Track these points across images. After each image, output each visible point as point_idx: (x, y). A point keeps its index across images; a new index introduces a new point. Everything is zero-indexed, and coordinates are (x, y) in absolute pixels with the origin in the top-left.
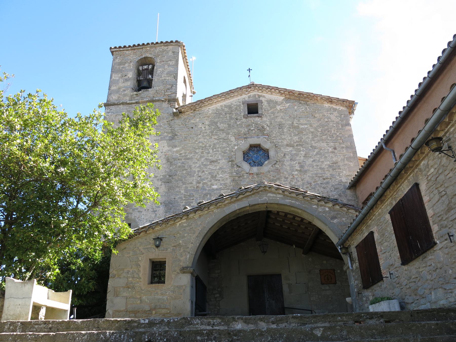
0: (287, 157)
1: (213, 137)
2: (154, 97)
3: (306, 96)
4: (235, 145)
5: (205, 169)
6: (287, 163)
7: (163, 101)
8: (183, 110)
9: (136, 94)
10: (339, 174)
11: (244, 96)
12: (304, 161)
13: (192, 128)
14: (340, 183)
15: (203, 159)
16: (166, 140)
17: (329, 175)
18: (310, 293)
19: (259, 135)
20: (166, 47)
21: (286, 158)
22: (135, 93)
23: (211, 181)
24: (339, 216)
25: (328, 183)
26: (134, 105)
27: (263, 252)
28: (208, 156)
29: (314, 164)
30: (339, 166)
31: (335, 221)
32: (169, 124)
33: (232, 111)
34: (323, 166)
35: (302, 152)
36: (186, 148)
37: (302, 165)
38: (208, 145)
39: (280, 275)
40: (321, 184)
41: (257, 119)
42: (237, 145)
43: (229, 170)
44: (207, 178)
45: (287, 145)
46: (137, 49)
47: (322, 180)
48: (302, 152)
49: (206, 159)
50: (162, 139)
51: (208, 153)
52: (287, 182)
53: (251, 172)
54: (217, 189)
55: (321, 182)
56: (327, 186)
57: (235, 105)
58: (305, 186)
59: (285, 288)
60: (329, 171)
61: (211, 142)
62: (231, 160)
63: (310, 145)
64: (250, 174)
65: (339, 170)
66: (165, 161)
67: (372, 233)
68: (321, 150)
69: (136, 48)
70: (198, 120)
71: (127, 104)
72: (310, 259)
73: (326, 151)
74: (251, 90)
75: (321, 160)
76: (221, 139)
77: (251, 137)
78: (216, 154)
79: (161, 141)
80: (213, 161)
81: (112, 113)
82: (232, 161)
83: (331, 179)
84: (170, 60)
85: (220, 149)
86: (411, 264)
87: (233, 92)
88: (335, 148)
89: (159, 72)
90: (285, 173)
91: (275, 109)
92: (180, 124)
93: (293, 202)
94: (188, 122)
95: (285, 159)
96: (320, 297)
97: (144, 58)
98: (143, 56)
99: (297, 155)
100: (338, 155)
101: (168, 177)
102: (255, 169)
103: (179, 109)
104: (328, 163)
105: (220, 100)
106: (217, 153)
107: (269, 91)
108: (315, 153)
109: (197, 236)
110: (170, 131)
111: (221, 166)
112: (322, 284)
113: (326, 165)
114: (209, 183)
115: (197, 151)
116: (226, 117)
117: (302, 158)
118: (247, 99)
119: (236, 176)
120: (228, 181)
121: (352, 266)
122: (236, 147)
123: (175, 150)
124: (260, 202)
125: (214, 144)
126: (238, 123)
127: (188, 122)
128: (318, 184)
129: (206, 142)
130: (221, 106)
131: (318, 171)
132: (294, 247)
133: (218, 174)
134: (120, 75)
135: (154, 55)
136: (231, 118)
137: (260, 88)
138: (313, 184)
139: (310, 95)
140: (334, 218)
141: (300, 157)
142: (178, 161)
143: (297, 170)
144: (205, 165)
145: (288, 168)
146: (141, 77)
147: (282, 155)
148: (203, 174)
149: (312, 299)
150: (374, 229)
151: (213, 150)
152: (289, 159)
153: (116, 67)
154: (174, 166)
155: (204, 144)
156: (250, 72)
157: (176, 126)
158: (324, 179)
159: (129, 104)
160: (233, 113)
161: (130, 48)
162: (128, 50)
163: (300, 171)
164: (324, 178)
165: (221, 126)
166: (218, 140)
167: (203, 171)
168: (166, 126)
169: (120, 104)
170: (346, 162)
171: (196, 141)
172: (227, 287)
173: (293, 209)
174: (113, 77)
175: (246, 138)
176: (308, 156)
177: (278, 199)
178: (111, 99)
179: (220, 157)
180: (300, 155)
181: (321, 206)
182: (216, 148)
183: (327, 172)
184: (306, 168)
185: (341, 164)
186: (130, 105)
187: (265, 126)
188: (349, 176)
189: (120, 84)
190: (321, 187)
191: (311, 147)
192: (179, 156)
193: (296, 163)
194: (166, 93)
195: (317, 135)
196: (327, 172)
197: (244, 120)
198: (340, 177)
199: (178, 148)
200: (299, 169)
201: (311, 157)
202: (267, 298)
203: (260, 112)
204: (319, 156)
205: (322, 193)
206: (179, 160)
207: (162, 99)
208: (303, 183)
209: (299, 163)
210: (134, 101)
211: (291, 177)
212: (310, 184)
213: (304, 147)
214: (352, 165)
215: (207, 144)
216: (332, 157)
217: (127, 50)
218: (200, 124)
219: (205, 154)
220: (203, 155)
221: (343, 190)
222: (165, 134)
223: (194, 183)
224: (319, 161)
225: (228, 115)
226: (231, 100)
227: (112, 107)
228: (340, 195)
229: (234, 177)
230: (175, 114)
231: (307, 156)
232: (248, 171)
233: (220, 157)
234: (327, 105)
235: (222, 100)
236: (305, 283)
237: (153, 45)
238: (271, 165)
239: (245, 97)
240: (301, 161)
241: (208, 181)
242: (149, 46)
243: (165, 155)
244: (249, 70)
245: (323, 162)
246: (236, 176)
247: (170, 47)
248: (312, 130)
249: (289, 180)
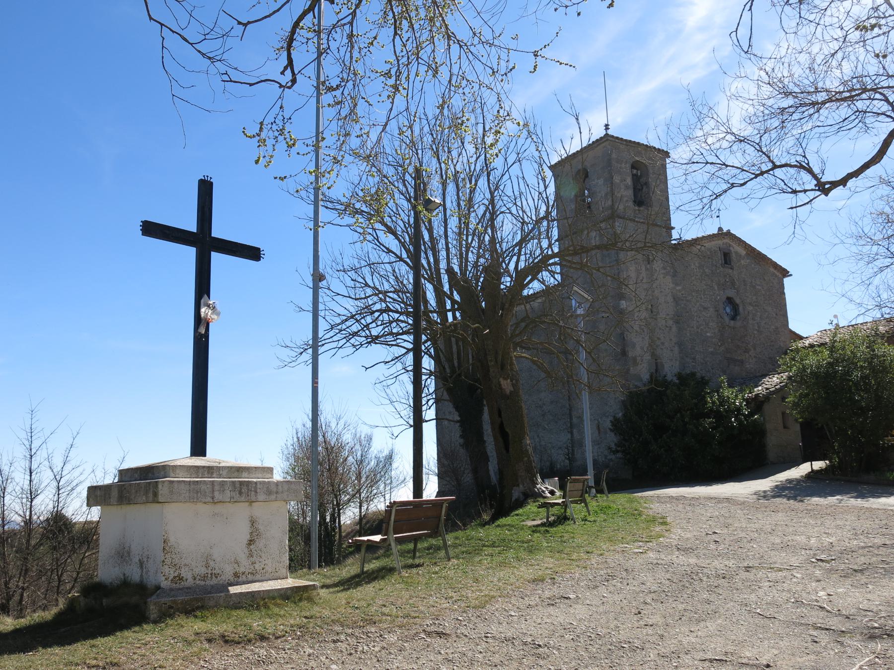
6: (751, 322)
15: (698, 304)
66: (672, 300)
114: (705, 330)
117: (759, 319)
120: (716, 331)
209: (757, 324)
212: (764, 344)
223: (695, 328)
234: (772, 269)
239: (719, 242)
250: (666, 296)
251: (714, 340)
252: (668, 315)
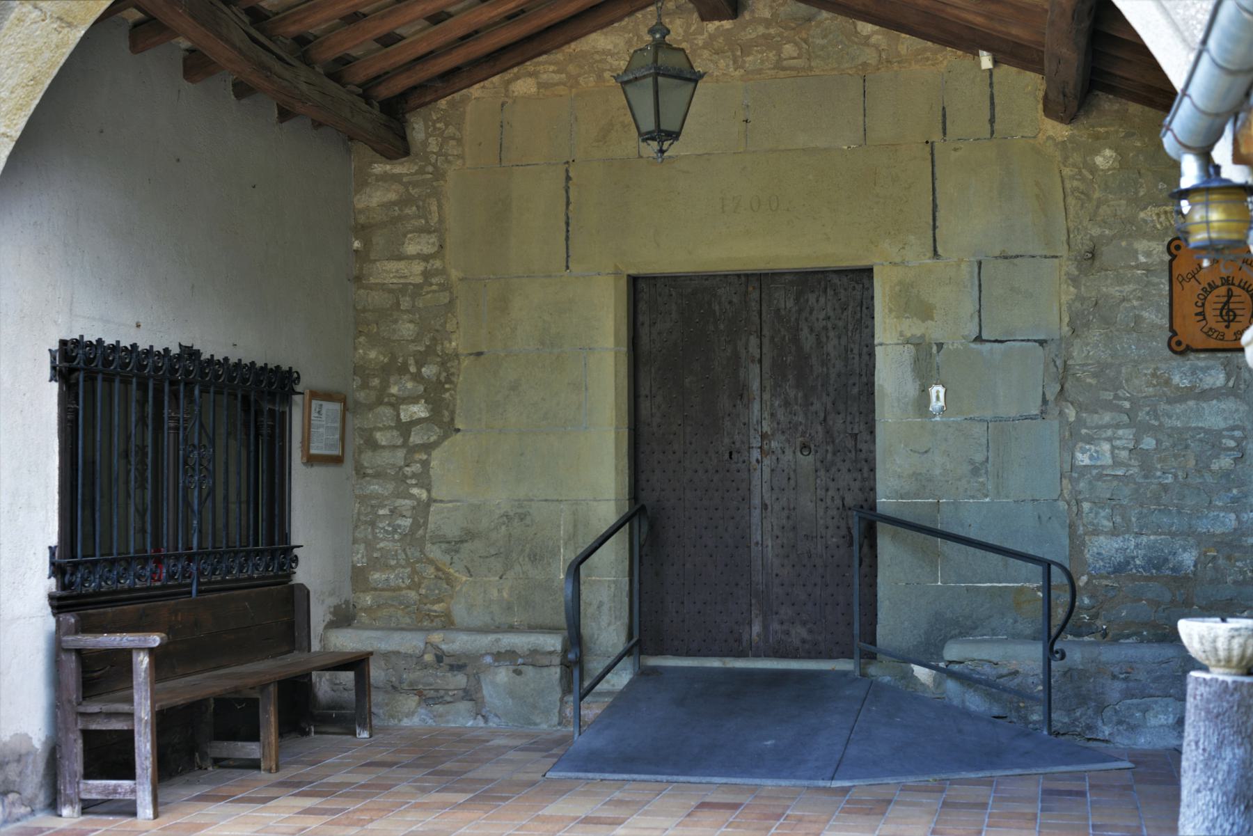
18: (1071, 413)
27: (647, 137)
72: (1104, 159)
96: (1149, 443)
112: (1179, 348)
132: (986, 61)
149: (1083, 459)
172: (479, 354)
202: (764, 436)
236: (1042, 343)
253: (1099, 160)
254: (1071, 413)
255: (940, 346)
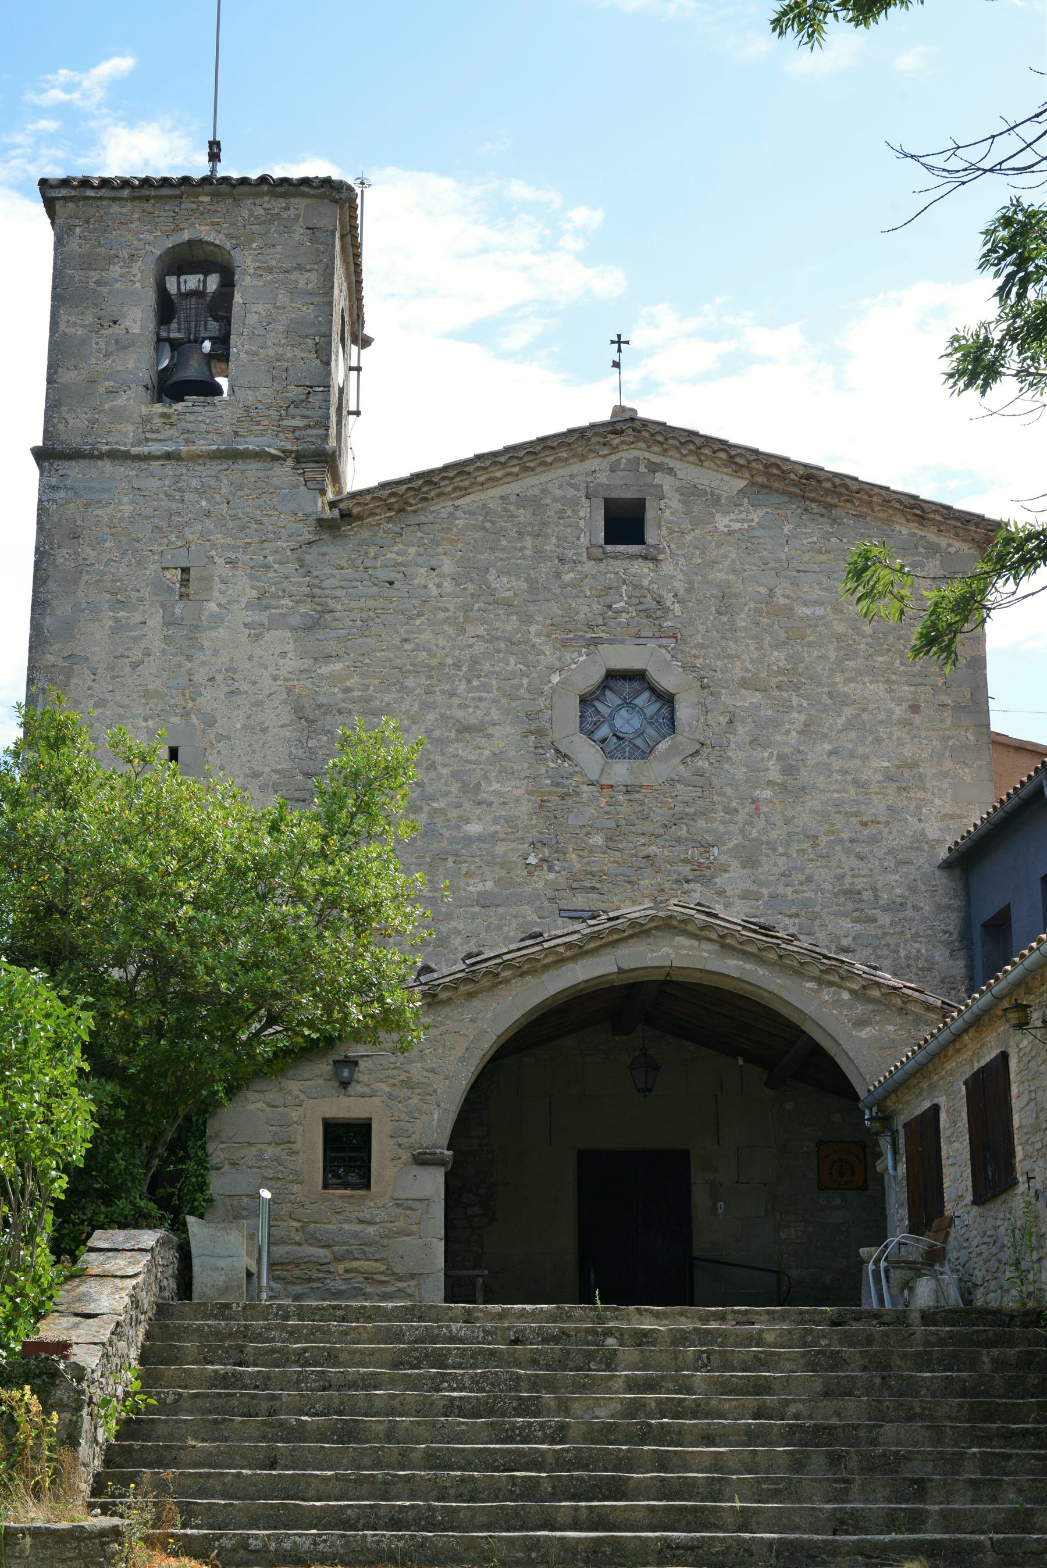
0: (740, 729)
1: (472, 629)
2: (236, 433)
3: (829, 485)
4: (553, 670)
5: (438, 759)
7: (274, 458)
8: (355, 511)
9: (164, 415)
10: (919, 808)
11: (593, 463)
12: (800, 752)
13: (391, 583)
14: (918, 841)
15: (430, 717)
16: (293, 629)
17: (882, 808)
18: (778, 1216)
19: (643, 634)
20: (282, 203)
21: (734, 733)
22: (159, 408)
23: (459, 806)
24: (878, 1018)
25: (874, 839)
26: (155, 465)
28: (450, 707)
29: (836, 764)
30: (921, 777)
31: (866, 1033)
32: (301, 561)
33: (544, 524)
34: (866, 774)
35: (795, 715)
36: (367, 665)
37: (791, 767)
38: (449, 661)
39: (686, 1153)
40: (851, 841)
41: (640, 568)
42: (561, 670)
43: (526, 766)
44: (447, 793)
45: (744, 684)
46: (155, 197)
47: (859, 827)
48: (795, 715)
49: (442, 716)
50: (276, 622)
51: (452, 694)
52: (733, 828)
53: (604, 782)
54: (480, 838)
55: (853, 835)
56: (871, 852)
57: (555, 500)
58: (796, 847)
59: (700, 1196)
60: (886, 795)
61: (461, 649)
62: (533, 728)
63: (826, 689)
64: (602, 787)
65: (921, 795)
66: (286, 715)
67: (935, 1109)
68: (864, 710)
69: (153, 192)
70: (412, 550)
71: (126, 456)
72: (789, 1106)
73: (882, 716)
74: (623, 442)
75: (861, 751)
76: (498, 638)
77: (611, 642)
78: (480, 699)
79: (272, 632)
80: (468, 729)
81: (71, 494)
82: (540, 733)
83: (887, 824)
84: (299, 268)
85: (494, 682)
86: (988, 1206)
87: (553, 448)
88: (915, 709)
89: (252, 319)
90: (729, 790)
91: (710, 527)
92: (343, 563)
93: (748, 966)
94: (376, 557)
95: (733, 738)
96: (810, 1229)
97: (190, 242)
98: (186, 236)
99: (775, 723)
100: (923, 734)
101: (300, 777)
102: (621, 771)
103: (343, 506)
104: (886, 764)
105: (499, 474)
106: (484, 695)
107: (691, 452)
108: (840, 722)
109: (462, 1059)
110: (306, 590)
111: (497, 751)
112: (822, 1187)
113: (875, 771)
115: (410, 682)
116: (522, 549)
118: (603, 478)
119: (551, 793)
120: (525, 807)
121: (895, 1168)
122: (556, 679)
123: (325, 670)
124: (650, 964)
125: (474, 661)
126: (568, 577)
127: (376, 557)
128: (841, 841)
129: (443, 648)
130: (502, 497)
131: (845, 791)
132: (740, 1062)
133: (486, 777)
134: (89, 319)
135: (229, 236)
136: (540, 554)
137: (660, 438)
138: (824, 838)
139: (845, 486)
140: (861, 1023)
141: (788, 732)
142: (339, 718)
143: (770, 783)
144: (438, 741)
145: (740, 773)
146: (174, 325)
147: (724, 720)
148: (432, 774)
149: (783, 1235)
150: (942, 1101)
151: (469, 681)
152: (748, 739)
153: (72, 277)
154: (325, 738)
155: (432, 656)
156: (619, 350)
157: (328, 571)
158: (864, 824)
159: (138, 458)
160: (549, 531)
161: (126, 193)
162: (121, 199)
163: (784, 787)
164: (865, 819)
165: (505, 585)
166: (486, 641)
167: (433, 766)
168: (290, 568)
169: (101, 456)
170: (948, 765)
171: (405, 640)
173: (744, 985)
174: (63, 326)
175: (595, 642)
176: (816, 733)
177: (706, 954)
178: (61, 426)
179: (495, 715)
180: (787, 726)
181: (831, 984)
182: (479, 676)
183: (875, 799)
184: (805, 776)
185: (928, 770)
186: (143, 465)
187: (669, 599)
188: (951, 817)
189: (93, 360)
190: (848, 851)
191: (830, 695)
192: (341, 696)
193: (770, 757)
194: (285, 423)
195: (857, 652)
196: (875, 799)
197: (589, 566)
198: (920, 820)
199: (339, 666)
200: (779, 779)
201: (825, 736)
203: (650, 537)
204: (853, 735)
205: (853, 876)
206: (340, 712)
207: (273, 451)
208: (790, 834)
209: (781, 758)
210: (156, 448)
211: (750, 808)
213: (806, 697)
214: (968, 778)
215: (446, 656)
216: (901, 743)
217: (114, 199)
218: (423, 570)
219: (439, 698)
220: (430, 699)
221: (926, 868)
222: (286, 601)
224: (852, 755)
225: (528, 541)
226: (544, 478)
227: (67, 464)
228: (912, 889)
229: (543, 794)
230: (322, 524)
231: (812, 733)
232: (594, 776)
233: (495, 715)
235: (508, 474)
236: (765, 1184)
237: (224, 188)
238: (679, 759)
240: (788, 750)
241: (448, 805)
242: (207, 188)
243: (289, 691)
244: (619, 342)
245: (865, 758)
246: (551, 793)
247: (299, 204)
248: (840, 628)
249: (740, 818)
250: (258, 704)
251: (501, 848)
252: (255, 775)
253: (787, 1106)
254: (778, 1216)
255: (721, 1185)
